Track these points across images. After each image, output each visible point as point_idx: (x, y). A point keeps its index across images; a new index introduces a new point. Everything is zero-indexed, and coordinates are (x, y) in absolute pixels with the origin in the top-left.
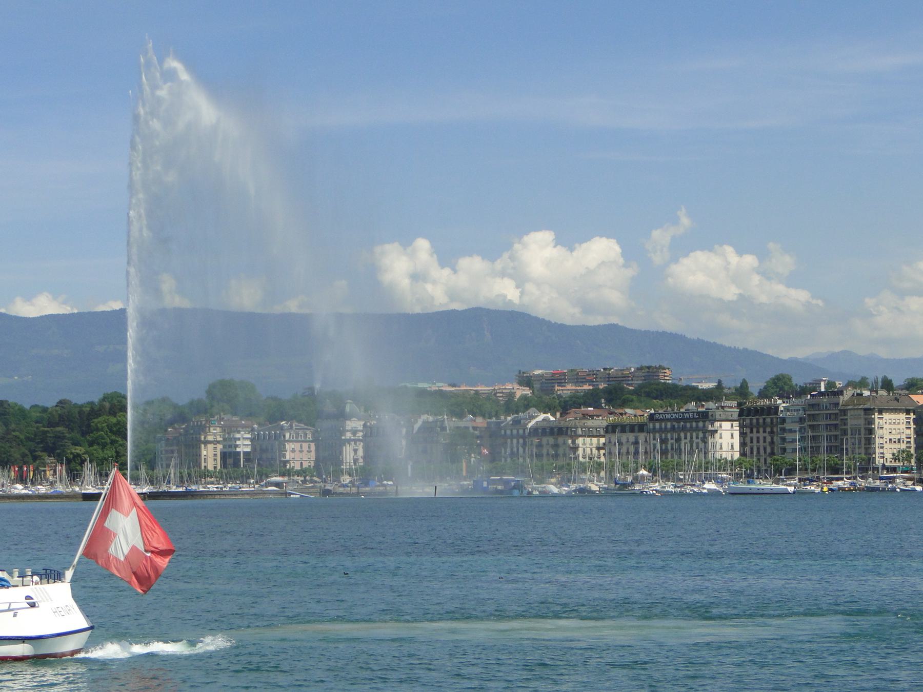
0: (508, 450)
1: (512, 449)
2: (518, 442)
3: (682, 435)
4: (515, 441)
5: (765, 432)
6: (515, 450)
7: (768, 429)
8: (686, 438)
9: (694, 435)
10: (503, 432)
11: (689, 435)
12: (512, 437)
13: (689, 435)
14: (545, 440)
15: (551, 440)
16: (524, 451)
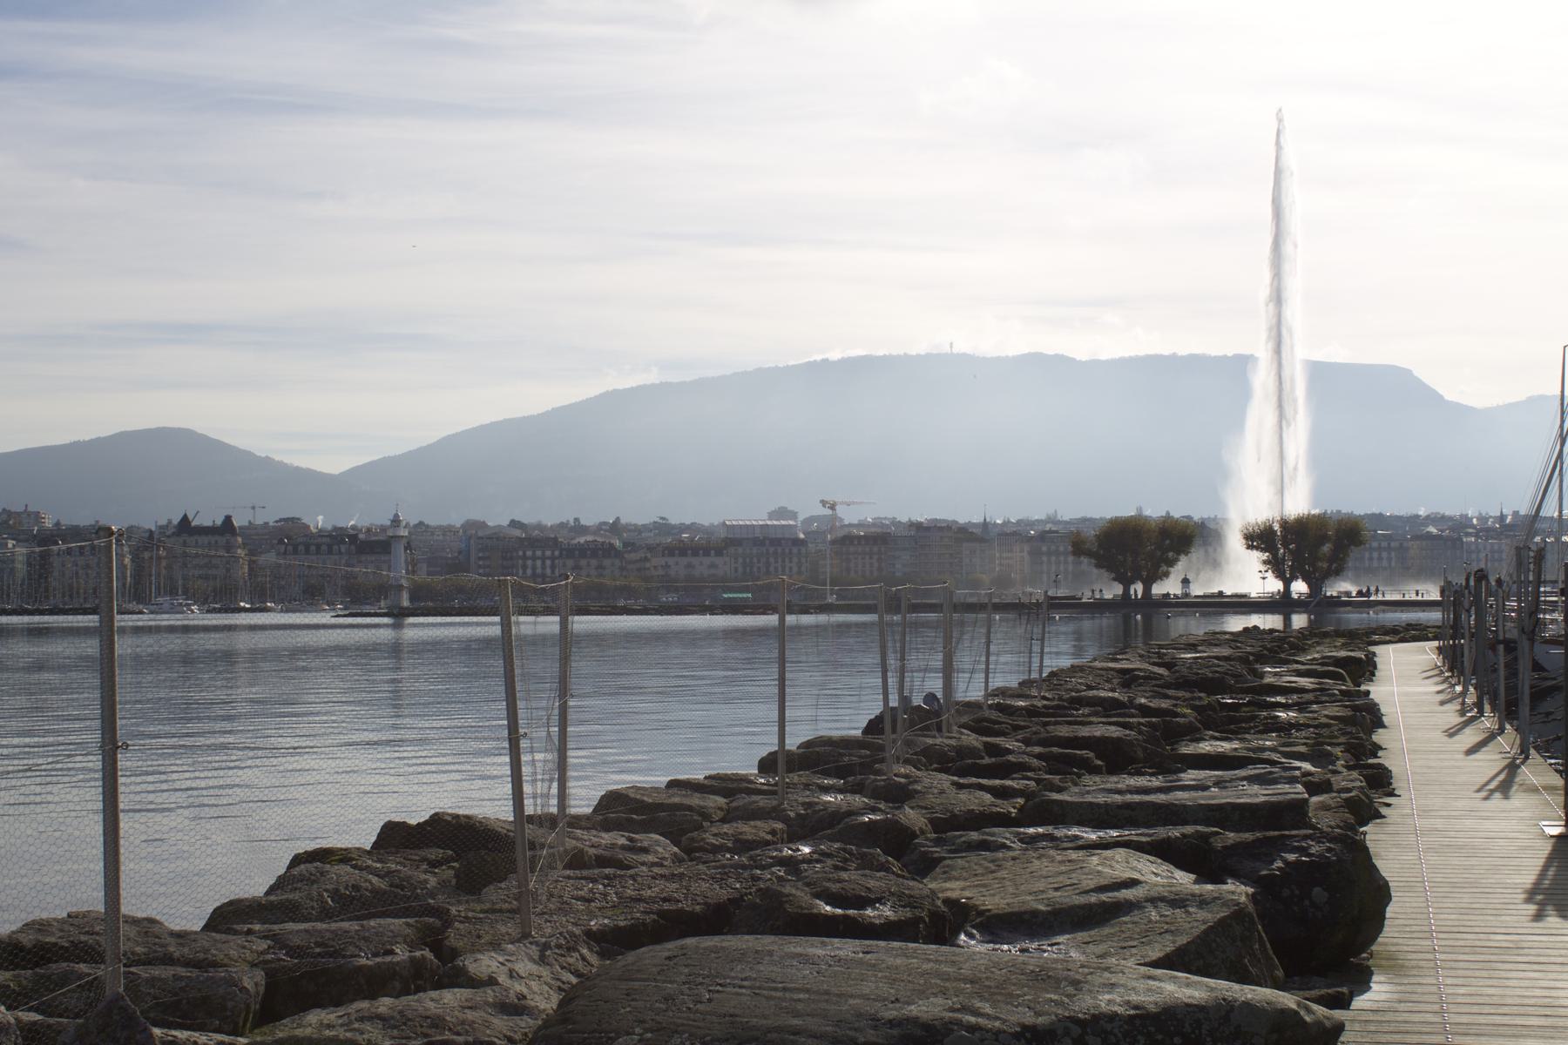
0: (529, 572)
1: (534, 568)
2: (543, 563)
3: (772, 560)
4: (539, 563)
5: (871, 558)
6: (539, 571)
7: (876, 557)
8: (776, 562)
9: (787, 560)
10: (521, 553)
11: (780, 560)
12: (534, 558)
13: (780, 560)
14: (583, 562)
15: (594, 562)
16: (553, 572)
